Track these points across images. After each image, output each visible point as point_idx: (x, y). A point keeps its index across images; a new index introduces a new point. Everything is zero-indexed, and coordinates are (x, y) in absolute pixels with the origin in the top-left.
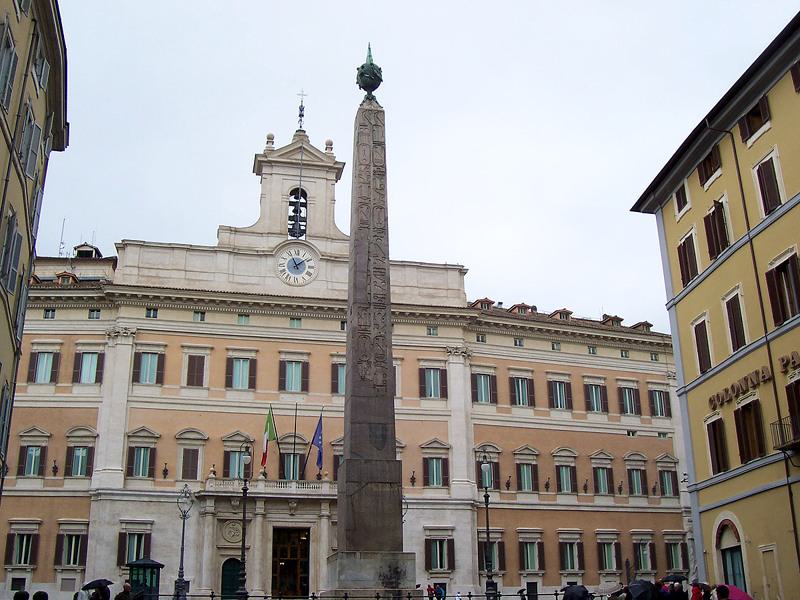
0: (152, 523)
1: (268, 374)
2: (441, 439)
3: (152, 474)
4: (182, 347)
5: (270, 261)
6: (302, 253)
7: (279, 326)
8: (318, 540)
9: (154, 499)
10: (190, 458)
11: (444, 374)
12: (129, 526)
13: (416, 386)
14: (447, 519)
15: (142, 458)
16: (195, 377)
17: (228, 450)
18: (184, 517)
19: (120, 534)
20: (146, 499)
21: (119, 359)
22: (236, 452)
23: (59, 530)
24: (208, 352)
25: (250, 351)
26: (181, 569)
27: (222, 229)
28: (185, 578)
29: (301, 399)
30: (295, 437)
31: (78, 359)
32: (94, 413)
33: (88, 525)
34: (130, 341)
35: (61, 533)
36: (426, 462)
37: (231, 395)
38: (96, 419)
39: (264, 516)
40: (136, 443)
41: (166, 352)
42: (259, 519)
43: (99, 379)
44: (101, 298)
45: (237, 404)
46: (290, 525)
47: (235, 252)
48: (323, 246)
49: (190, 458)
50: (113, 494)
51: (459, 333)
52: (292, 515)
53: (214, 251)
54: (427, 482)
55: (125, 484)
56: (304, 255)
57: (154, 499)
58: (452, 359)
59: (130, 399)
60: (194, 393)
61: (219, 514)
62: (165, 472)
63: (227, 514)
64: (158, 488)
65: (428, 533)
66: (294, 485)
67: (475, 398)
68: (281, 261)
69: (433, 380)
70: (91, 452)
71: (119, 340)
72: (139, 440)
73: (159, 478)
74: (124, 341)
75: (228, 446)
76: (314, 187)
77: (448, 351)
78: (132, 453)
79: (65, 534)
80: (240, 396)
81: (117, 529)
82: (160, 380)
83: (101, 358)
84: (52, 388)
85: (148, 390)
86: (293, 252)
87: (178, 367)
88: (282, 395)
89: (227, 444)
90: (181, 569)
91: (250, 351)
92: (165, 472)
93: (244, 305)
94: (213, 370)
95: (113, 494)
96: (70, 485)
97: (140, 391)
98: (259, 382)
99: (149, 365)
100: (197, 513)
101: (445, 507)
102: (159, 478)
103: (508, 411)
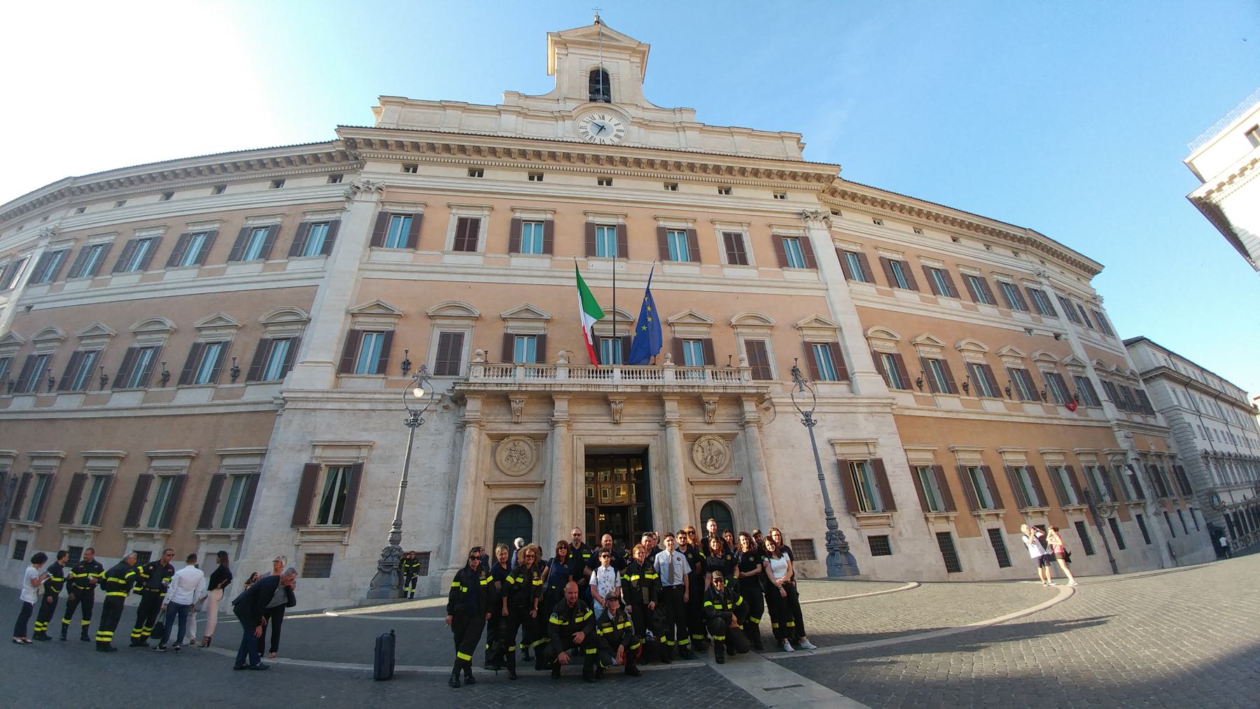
0: (370, 446)
1: (569, 236)
2: (823, 317)
3: (382, 368)
4: (449, 206)
5: (568, 123)
6: (607, 117)
7: (583, 185)
8: (666, 466)
9: (380, 406)
10: (450, 348)
11: (805, 245)
12: (329, 453)
13: (771, 255)
14: (865, 427)
15: (369, 350)
16: (467, 236)
17: (510, 331)
18: (415, 423)
19: (310, 472)
20: (366, 406)
21: (358, 221)
22: (527, 341)
23: (220, 467)
24: (486, 213)
25: (545, 211)
26: (398, 525)
27: (507, 93)
28: (407, 546)
29: (621, 266)
30: (614, 313)
31: (304, 231)
32: (308, 294)
33: (262, 455)
34: (375, 197)
35: (222, 471)
36: (808, 348)
37: (517, 261)
38: (312, 300)
39: (569, 424)
40: (363, 324)
41: (427, 213)
42: (561, 430)
43: (327, 249)
44: (344, 156)
45: (526, 273)
46: (614, 441)
47: (522, 113)
48: (632, 112)
49: (450, 348)
50: (307, 400)
51: (813, 198)
52: (616, 423)
53: (498, 110)
54: (815, 375)
55: (336, 386)
56: (610, 121)
57: (380, 406)
58: (810, 223)
59: (363, 266)
60: (465, 258)
61: (489, 426)
62: (406, 366)
63: (506, 427)
64: (389, 390)
65: (838, 450)
66: (617, 372)
67: (847, 275)
68: (582, 124)
69: (792, 250)
70: (294, 344)
71: (358, 197)
72: (371, 319)
73: (395, 374)
74: (365, 197)
75: (512, 328)
76: (619, 69)
77: (804, 216)
78: (353, 340)
79: (228, 473)
80: (530, 264)
81: (305, 458)
82: (413, 242)
83: (334, 226)
84: (259, 267)
85: (393, 256)
86: (596, 116)
87: (443, 227)
88: (591, 263)
89: (511, 324)
90: (398, 525)
91: (545, 211)
92: (406, 366)
93: (537, 159)
94: (491, 233)
95: (307, 400)
96: (255, 394)
97: (381, 255)
98: (556, 248)
99: (399, 229)
100: (452, 428)
101: (853, 409)
102: (395, 374)
103: (892, 295)
